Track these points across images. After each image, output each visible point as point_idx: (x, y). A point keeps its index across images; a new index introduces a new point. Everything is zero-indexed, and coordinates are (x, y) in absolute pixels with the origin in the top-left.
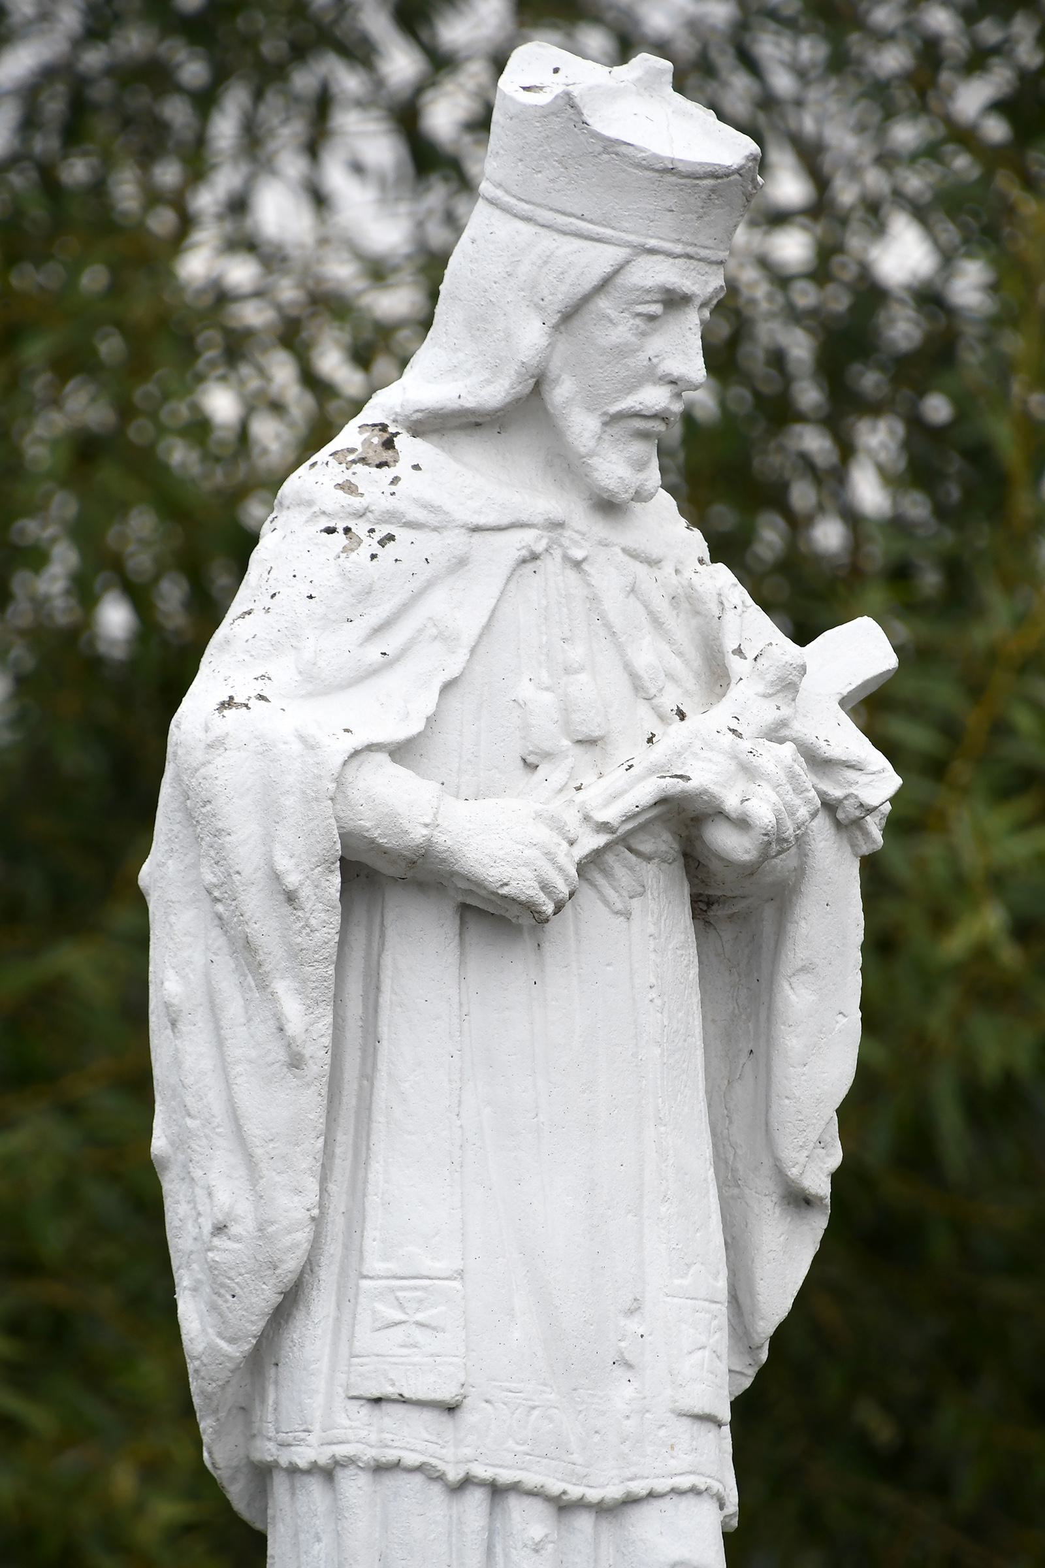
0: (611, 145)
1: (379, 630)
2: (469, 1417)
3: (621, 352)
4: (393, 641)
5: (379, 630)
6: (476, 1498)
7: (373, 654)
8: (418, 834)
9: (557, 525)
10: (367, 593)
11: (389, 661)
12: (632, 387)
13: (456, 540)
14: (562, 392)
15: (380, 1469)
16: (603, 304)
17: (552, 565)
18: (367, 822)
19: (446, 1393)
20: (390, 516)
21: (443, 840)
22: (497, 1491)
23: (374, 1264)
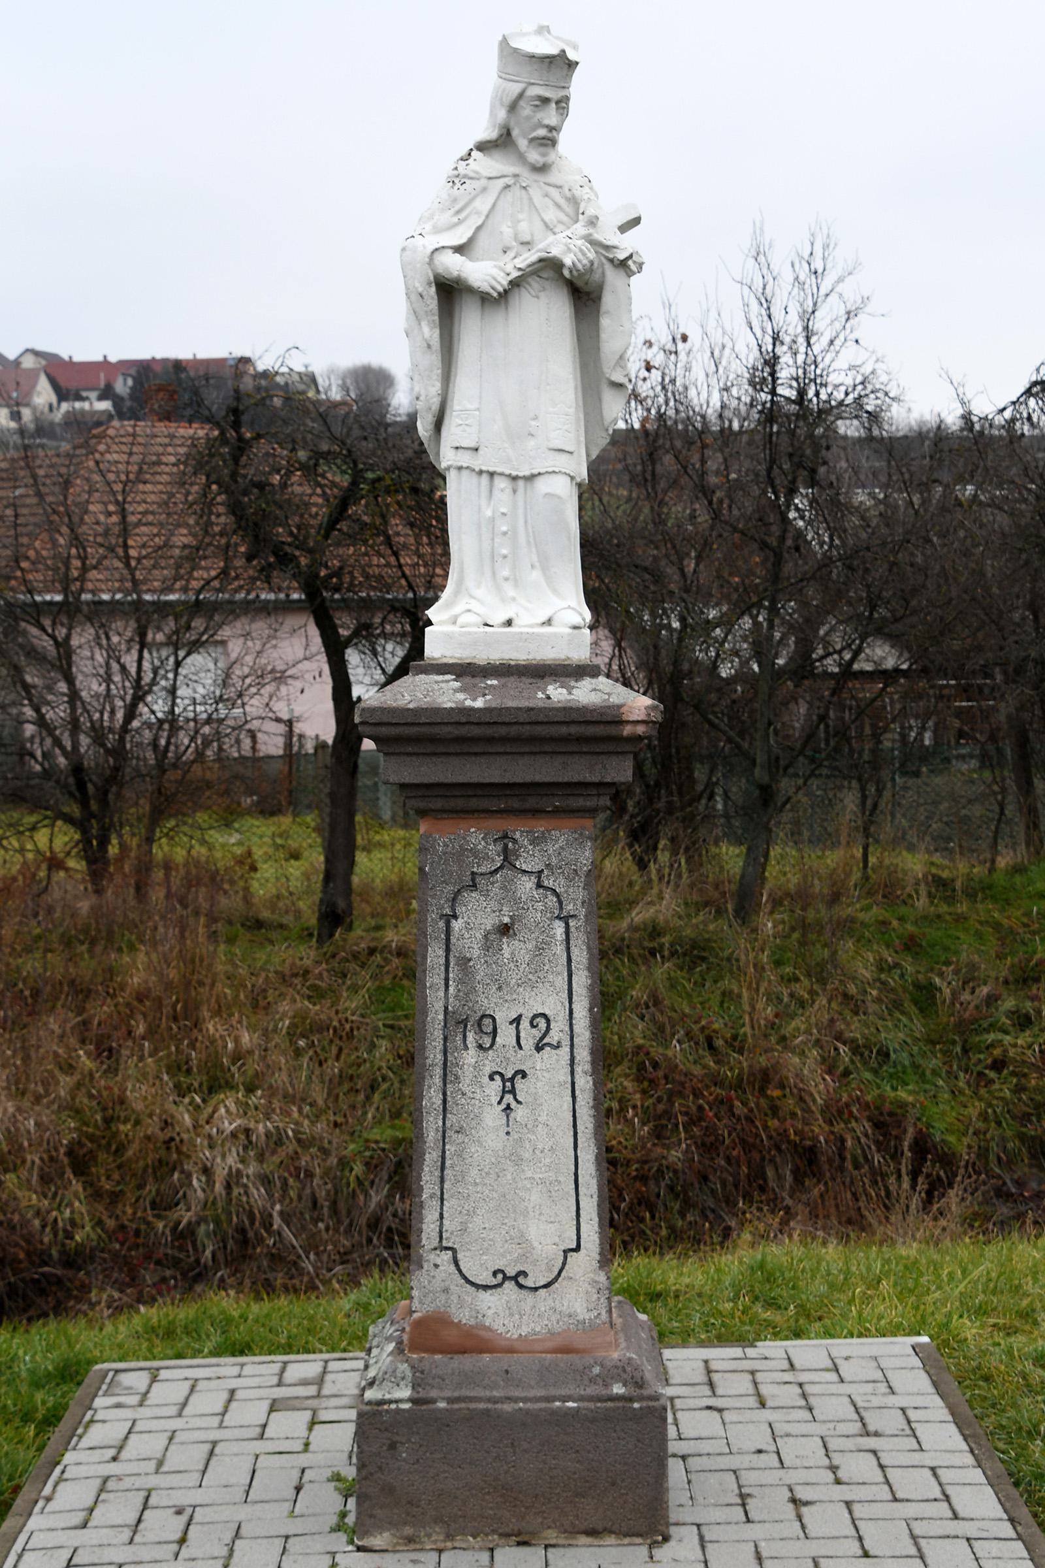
0: (516, 50)
1: (458, 212)
2: (480, 452)
3: (528, 118)
4: (462, 216)
5: (458, 212)
6: (485, 479)
7: (455, 220)
8: (455, 274)
9: (516, 176)
10: (455, 200)
11: (460, 222)
12: (535, 128)
13: (483, 182)
14: (515, 133)
15: (460, 468)
16: (522, 103)
17: (516, 189)
18: (440, 270)
19: (473, 445)
20: (465, 176)
21: (463, 275)
22: (492, 474)
23: (456, 407)
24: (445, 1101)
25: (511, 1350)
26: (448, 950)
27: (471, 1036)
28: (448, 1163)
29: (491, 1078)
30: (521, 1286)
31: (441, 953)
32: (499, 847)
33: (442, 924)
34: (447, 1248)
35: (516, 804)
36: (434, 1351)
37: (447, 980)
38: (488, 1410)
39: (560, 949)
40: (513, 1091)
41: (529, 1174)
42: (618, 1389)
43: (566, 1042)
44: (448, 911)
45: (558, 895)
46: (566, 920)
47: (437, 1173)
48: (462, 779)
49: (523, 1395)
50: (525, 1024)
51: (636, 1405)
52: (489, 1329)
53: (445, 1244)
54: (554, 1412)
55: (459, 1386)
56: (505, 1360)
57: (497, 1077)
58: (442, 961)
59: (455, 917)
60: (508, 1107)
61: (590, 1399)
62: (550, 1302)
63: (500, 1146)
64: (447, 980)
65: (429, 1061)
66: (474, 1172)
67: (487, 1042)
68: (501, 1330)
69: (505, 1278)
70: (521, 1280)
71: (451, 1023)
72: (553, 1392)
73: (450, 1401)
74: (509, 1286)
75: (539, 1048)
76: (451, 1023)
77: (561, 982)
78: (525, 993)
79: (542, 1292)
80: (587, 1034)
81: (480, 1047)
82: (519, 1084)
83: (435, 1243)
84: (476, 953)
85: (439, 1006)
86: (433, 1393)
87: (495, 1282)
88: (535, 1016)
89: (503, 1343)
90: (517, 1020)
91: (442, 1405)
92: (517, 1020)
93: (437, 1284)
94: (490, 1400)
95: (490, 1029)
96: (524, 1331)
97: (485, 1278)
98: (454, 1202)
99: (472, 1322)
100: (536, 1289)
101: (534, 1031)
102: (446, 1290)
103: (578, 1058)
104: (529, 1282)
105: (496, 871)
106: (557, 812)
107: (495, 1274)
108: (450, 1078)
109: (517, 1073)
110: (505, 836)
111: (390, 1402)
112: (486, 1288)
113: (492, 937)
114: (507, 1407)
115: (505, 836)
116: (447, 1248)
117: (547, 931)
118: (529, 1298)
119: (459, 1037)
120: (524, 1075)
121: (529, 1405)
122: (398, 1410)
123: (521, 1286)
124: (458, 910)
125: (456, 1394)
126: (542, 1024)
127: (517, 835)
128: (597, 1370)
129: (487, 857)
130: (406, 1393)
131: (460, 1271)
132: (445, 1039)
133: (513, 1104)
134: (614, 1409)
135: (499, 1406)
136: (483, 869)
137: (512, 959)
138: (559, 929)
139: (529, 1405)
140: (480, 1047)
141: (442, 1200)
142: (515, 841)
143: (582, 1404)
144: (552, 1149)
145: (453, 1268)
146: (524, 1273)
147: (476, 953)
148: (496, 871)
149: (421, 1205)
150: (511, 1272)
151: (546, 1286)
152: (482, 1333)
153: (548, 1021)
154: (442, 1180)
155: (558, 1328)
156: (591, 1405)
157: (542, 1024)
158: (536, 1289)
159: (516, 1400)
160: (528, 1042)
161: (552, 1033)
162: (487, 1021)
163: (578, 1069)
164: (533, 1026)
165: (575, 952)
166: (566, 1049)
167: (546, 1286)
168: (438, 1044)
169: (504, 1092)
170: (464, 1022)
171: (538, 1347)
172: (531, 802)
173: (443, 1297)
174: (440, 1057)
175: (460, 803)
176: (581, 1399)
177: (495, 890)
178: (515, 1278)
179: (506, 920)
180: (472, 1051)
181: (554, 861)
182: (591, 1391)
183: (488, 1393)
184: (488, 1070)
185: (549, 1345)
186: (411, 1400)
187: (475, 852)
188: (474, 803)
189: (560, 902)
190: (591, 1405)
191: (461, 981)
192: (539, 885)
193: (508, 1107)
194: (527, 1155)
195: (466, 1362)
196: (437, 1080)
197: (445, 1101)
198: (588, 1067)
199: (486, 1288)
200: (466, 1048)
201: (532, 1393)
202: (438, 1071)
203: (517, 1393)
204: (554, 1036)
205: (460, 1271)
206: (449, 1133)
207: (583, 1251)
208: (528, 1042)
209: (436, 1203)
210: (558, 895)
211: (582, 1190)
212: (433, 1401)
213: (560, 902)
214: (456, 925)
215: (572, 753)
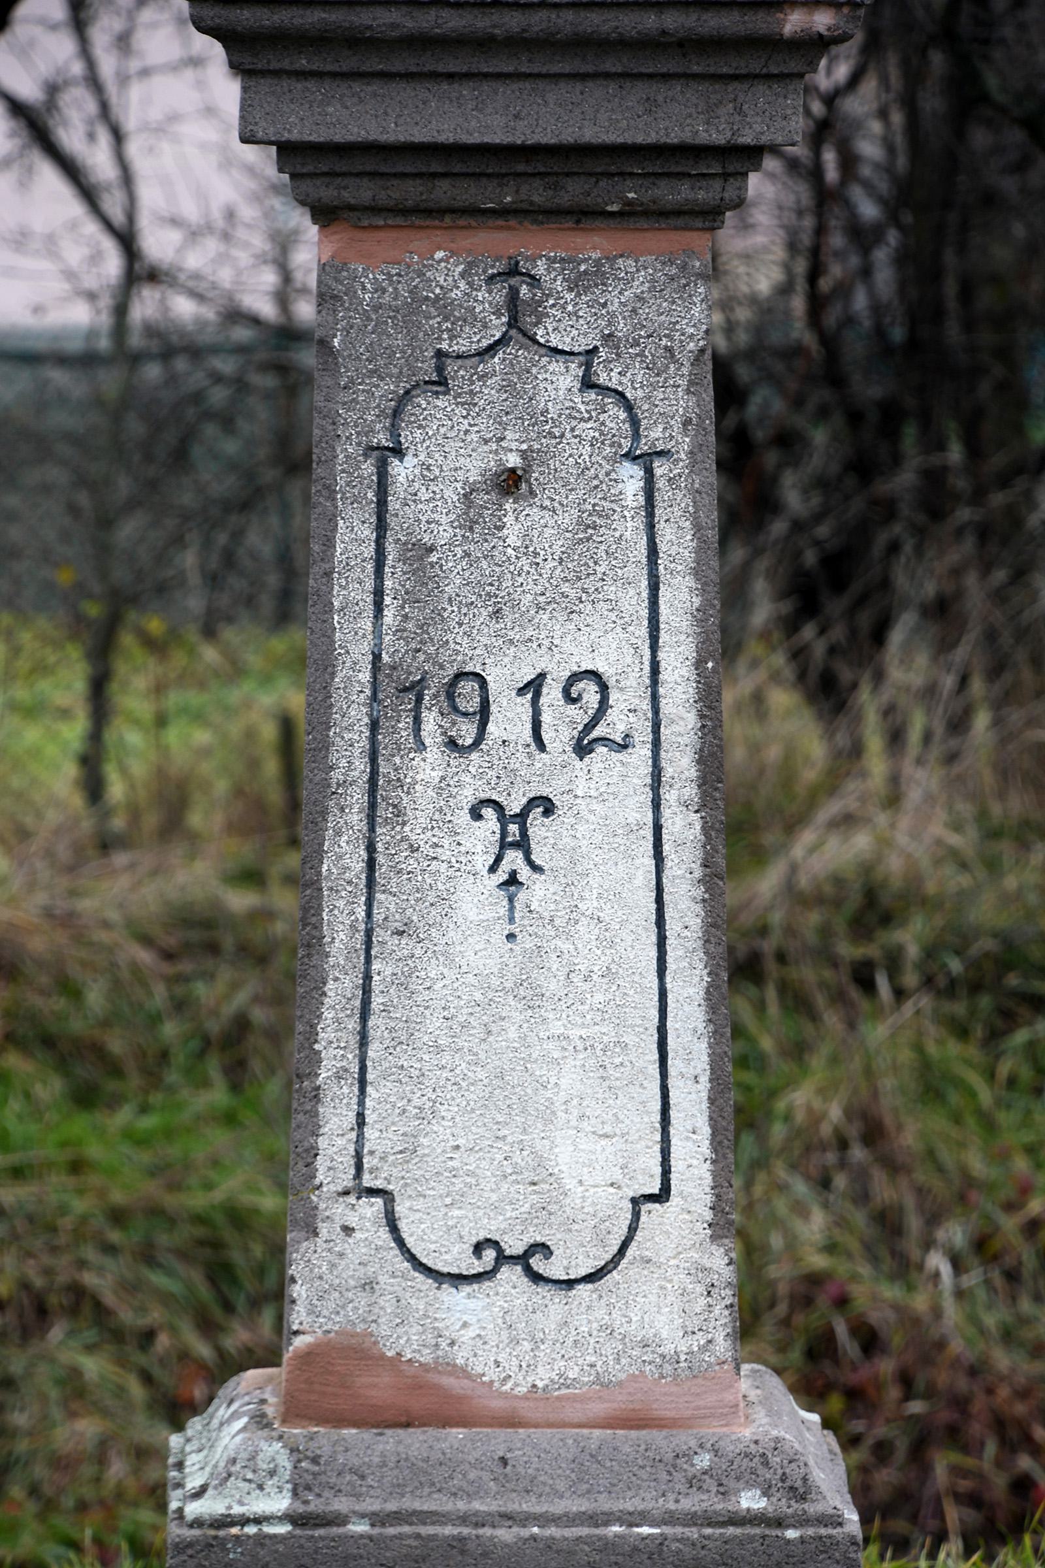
24: (371, 864)
25: (511, 1421)
26: (381, 527)
27: (431, 721)
28: (377, 1001)
29: (476, 815)
30: (537, 1278)
31: (368, 532)
32: (499, 295)
33: (368, 468)
34: (372, 1192)
35: (538, 195)
36: (340, 1421)
37: (379, 593)
38: (462, 1539)
39: (632, 529)
40: (523, 844)
41: (557, 1028)
42: (751, 1501)
43: (643, 735)
44: (382, 438)
45: (629, 407)
46: (646, 460)
47: (353, 1024)
48: (419, 135)
49: (538, 1509)
50: (552, 694)
51: (791, 1534)
52: (463, 1372)
53: (367, 1181)
54: (607, 1546)
55: (399, 1489)
56: (499, 1440)
57: (489, 813)
58: (369, 550)
59: (399, 452)
60: (513, 880)
61: (692, 1519)
62: (600, 1313)
63: (493, 965)
64: (379, 593)
65: (336, 776)
66: (434, 1023)
67: (467, 732)
68: (492, 1374)
69: (502, 1259)
70: (537, 1263)
71: (388, 689)
72: (605, 1504)
73: (377, 1519)
74: (511, 1275)
75: (582, 749)
76: (388, 689)
77: (634, 600)
78: (553, 625)
79: (583, 1290)
80: (691, 719)
81: (452, 744)
82: (537, 826)
83: (346, 1179)
84: (444, 534)
85: (361, 651)
86: (341, 1505)
87: (477, 1267)
88: (575, 678)
89: (497, 1404)
90: (535, 686)
91: (359, 1528)
92: (535, 686)
93: (349, 1272)
94: (464, 1519)
95: (473, 705)
96: (542, 1377)
97: (456, 1258)
98: (388, 1087)
99: (426, 1357)
100: (570, 1284)
101: (572, 710)
102: (369, 1285)
103: (668, 771)
104: (554, 1269)
105: (491, 349)
106: (630, 215)
107: (478, 1249)
108: (383, 812)
109: (532, 802)
110: (513, 271)
111: (244, 1521)
112: (458, 1279)
113: (481, 499)
114: (505, 1534)
115: (513, 271)
116: (372, 1192)
117: (603, 486)
118: (554, 1303)
119: (405, 723)
120: (549, 807)
121: (552, 1531)
122: (261, 1539)
123: (537, 1278)
124: (406, 438)
125: (392, 1506)
126: (590, 694)
127: (540, 268)
128: (704, 1461)
129: (470, 318)
130: (278, 1503)
131: (400, 1243)
132: (374, 726)
133: (524, 873)
134: (741, 1542)
135: (487, 1531)
136: (462, 345)
137: (525, 550)
138: (631, 480)
139: (552, 1531)
140: (452, 744)
141: (363, 1083)
142: (534, 281)
143: (668, 1530)
144: (607, 973)
145: (384, 1235)
146: (542, 1248)
147: (444, 534)
148: (491, 349)
149: (316, 1095)
150: (514, 1246)
151: (590, 1278)
152: (447, 1381)
153: (604, 688)
154: (363, 1041)
155: (618, 1372)
156: (693, 1533)
157: (590, 694)
158: (570, 1284)
159: (525, 1519)
160: (558, 736)
161: (612, 715)
162: (468, 687)
163: (670, 797)
164: (570, 699)
165: (667, 535)
166: (642, 752)
167: (590, 1278)
168: (360, 737)
169: (504, 845)
170: (416, 689)
171: (573, 1413)
172: (573, 192)
173: (362, 1300)
174: (361, 766)
175: (412, 192)
176: (670, 1519)
177: (489, 392)
178: (523, 1259)
179: (513, 460)
180: (434, 753)
181: (622, 328)
182: (691, 1503)
183: (461, 1505)
184: (468, 796)
185: (598, 1409)
186: (289, 1518)
187: (443, 306)
188: (443, 192)
189: (635, 422)
190: (693, 1533)
191: (409, 598)
192: (588, 384)
193: (513, 880)
194: (553, 987)
195: (415, 1441)
196: (356, 818)
197: (371, 864)
198: (691, 792)
199: (458, 1279)
200: (421, 746)
201: (559, 1507)
202: (357, 797)
203: (530, 1505)
204: (616, 724)
205: (400, 1243)
206: (379, 935)
207: (675, 1200)
208: (558, 736)
209: (349, 1090)
210: (629, 407)
211: (675, 1065)
212: (339, 1520)
213: (635, 422)
214: (402, 471)
215: (666, 77)
